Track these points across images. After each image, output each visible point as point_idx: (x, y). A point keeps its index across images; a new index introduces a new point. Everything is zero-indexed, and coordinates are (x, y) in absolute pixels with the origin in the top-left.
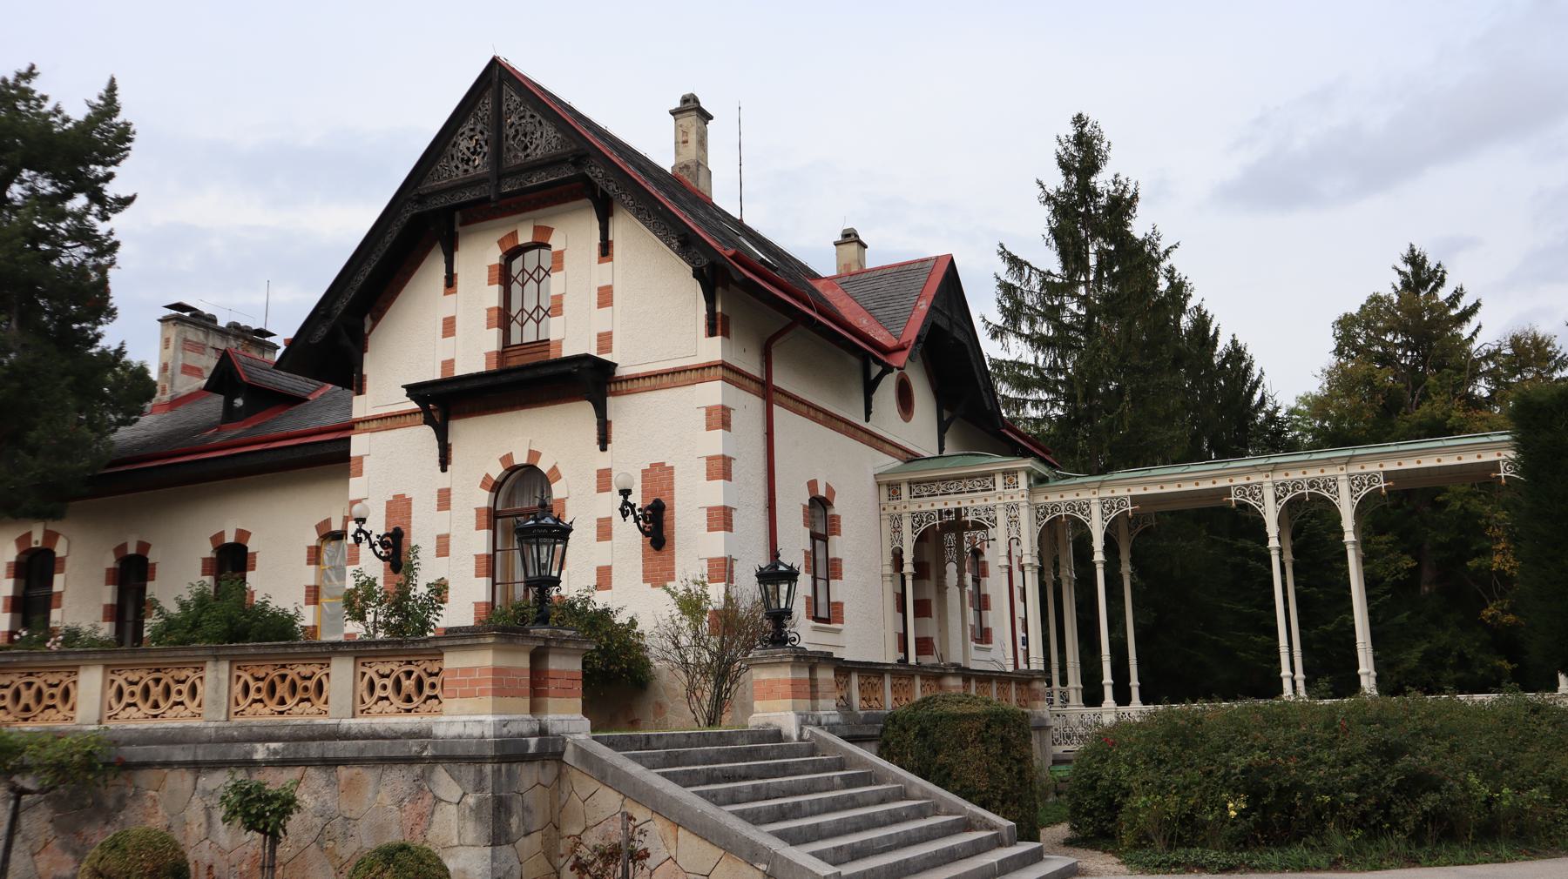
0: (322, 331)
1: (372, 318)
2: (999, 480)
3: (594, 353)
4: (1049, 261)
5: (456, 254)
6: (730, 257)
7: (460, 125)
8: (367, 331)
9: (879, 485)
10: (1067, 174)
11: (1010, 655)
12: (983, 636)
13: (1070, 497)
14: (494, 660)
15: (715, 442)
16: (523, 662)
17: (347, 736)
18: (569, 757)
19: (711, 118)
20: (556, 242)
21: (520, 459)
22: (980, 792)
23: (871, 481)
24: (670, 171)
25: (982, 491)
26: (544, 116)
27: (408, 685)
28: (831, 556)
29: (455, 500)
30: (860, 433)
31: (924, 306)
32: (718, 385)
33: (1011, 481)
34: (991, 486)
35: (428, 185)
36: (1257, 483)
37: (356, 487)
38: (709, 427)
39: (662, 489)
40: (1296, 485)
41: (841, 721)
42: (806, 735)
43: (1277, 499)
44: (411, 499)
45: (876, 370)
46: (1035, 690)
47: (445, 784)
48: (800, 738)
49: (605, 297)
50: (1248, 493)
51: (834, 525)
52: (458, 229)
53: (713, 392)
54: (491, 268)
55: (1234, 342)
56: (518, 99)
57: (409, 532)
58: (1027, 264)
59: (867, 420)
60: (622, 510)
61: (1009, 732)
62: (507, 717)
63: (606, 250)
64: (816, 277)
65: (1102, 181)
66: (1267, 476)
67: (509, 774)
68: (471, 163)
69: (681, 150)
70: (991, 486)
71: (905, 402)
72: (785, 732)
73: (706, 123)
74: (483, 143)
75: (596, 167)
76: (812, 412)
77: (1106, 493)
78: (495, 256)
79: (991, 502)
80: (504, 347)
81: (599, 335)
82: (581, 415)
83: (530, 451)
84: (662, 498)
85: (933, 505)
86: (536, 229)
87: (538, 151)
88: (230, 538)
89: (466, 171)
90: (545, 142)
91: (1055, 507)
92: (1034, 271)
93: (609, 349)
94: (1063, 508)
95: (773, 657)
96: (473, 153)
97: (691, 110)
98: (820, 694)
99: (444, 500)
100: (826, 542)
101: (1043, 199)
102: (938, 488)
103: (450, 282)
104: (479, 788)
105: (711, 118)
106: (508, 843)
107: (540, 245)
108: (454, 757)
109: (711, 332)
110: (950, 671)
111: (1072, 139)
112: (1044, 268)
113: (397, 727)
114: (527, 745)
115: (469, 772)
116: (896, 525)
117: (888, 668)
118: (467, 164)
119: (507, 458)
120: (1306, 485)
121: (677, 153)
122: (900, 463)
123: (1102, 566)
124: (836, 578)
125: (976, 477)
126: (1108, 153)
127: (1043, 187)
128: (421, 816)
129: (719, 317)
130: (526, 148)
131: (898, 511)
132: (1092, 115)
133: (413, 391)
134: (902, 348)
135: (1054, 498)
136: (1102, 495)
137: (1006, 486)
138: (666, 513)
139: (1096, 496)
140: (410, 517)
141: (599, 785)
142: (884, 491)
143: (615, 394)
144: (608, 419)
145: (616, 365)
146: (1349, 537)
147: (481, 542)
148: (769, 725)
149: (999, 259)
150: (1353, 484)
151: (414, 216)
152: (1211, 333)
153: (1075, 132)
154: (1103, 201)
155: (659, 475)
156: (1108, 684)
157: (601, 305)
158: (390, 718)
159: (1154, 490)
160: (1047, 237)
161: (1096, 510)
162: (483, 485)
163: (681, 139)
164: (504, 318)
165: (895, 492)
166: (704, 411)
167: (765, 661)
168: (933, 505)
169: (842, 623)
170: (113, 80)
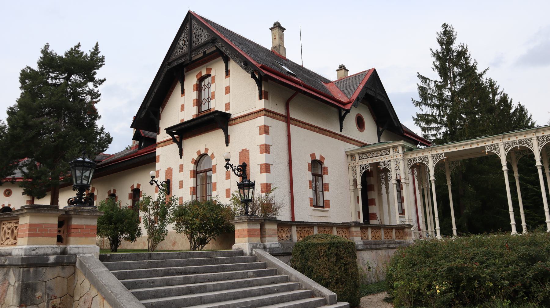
0: (144, 113)
1: (162, 108)
2: (391, 150)
3: (224, 111)
4: (436, 77)
5: (184, 82)
6: (260, 67)
7: (180, 37)
8: (160, 113)
9: (348, 155)
10: (441, 45)
11: (414, 218)
12: (402, 212)
13: (420, 155)
14: (30, 220)
15: (262, 139)
16: (258, 227)
18: (77, 265)
19: (285, 29)
20: (213, 73)
22: (325, 279)
23: (344, 154)
24: (270, 49)
25: (385, 155)
26: (204, 28)
28: (324, 182)
29: (185, 168)
30: (337, 136)
31: (361, 87)
33: (396, 150)
34: (389, 153)
35: (173, 58)
36: (497, 144)
39: (246, 159)
40: (513, 143)
41: (280, 247)
42: (254, 253)
43: (505, 150)
44: (172, 169)
45: (343, 112)
46: (406, 232)
48: (251, 254)
49: (228, 90)
50: (492, 148)
51: (325, 171)
52: (185, 73)
53: (261, 120)
54: (194, 85)
55: (519, 105)
56: (196, 24)
57: (172, 181)
58: (428, 79)
59: (341, 131)
60: (226, 167)
61: (340, 251)
62: (37, 246)
63: (227, 73)
64: (327, 81)
65: (455, 46)
66: (501, 141)
67: (36, 273)
68: (183, 49)
69: (274, 42)
70: (389, 153)
71: (360, 124)
72: (245, 251)
73: (283, 32)
74: (186, 41)
75: (219, 42)
76: (312, 128)
77: (434, 152)
79: (389, 159)
80: (199, 113)
81: (226, 104)
82: (220, 133)
83: (205, 148)
84: (245, 162)
85: (367, 162)
86: (207, 69)
87: (202, 41)
88: (135, 187)
89: (182, 52)
90: (204, 36)
91: (414, 159)
92: (430, 81)
94: (418, 160)
95: (240, 220)
96: (184, 46)
97: (278, 27)
98: (267, 235)
99: (181, 168)
100: (322, 177)
101: (433, 55)
102: (369, 155)
105: (285, 29)
106: (32, 304)
107: (208, 75)
109: (261, 98)
110: (352, 225)
111: (442, 33)
112: (434, 80)
113: (7, 251)
114: (48, 259)
116: (354, 170)
117: (315, 224)
118: (182, 49)
120: (518, 143)
121: (273, 43)
122: (358, 147)
123: (434, 182)
124: (326, 191)
125: (383, 150)
126: (456, 36)
127: (432, 51)
128: (4, 291)
129: (263, 92)
130: (199, 40)
131: (355, 165)
132: (449, 23)
134: (350, 102)
135: (414, 156)
136: (432, 154)
137: (394, 152)
138: (247, 167)
139: (430, 154)
140: (172, 175)
142: (349, 157)
143: (231, 125)
144: (229, 134)
145: (231, 114)
146: (538, 163)
148: (239, 248)
150: (539, 141)
151: (168, 70)
152: (509, 102)
153: (443, 30)
154: (455, 54)
155: (244, 153)
156: (438, 229)
157: (226, 93)
160: (433, 68)
161: (430, 160)
163: (273, 38)
164: (199, 103)
165: (353, 158)
166: (259, 128)
167: (238, 221)
168: (367, 162)
169: (329, 208)
170: (97, 43)
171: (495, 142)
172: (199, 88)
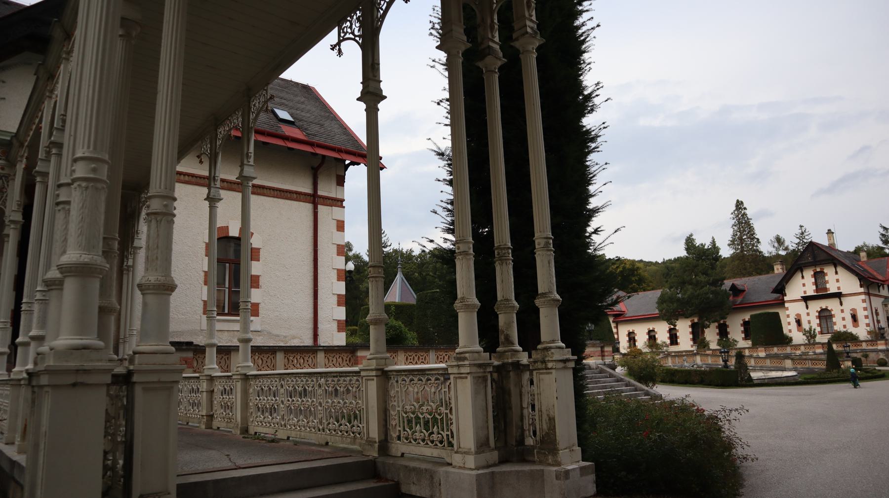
15: (865, 305)
21: (824, 307)
32: (864, 296)
37: (788, 312)
47: (880, 353)
49: (838, 281)
53: (863, 297)
54: (812, 275)
63: (836, 273)
78: (812, 273)
93: (840, 290)
97: (830, 232)
99: (808, 314)
103: (803, 277)
104: (885, 353)
108: (881, 351)
119: (821, 308)
133: (802, 297)
142: (884, 306)
147: (818, 321)
149: (880, 228)
170: (713, 237)
172: (816, 275)
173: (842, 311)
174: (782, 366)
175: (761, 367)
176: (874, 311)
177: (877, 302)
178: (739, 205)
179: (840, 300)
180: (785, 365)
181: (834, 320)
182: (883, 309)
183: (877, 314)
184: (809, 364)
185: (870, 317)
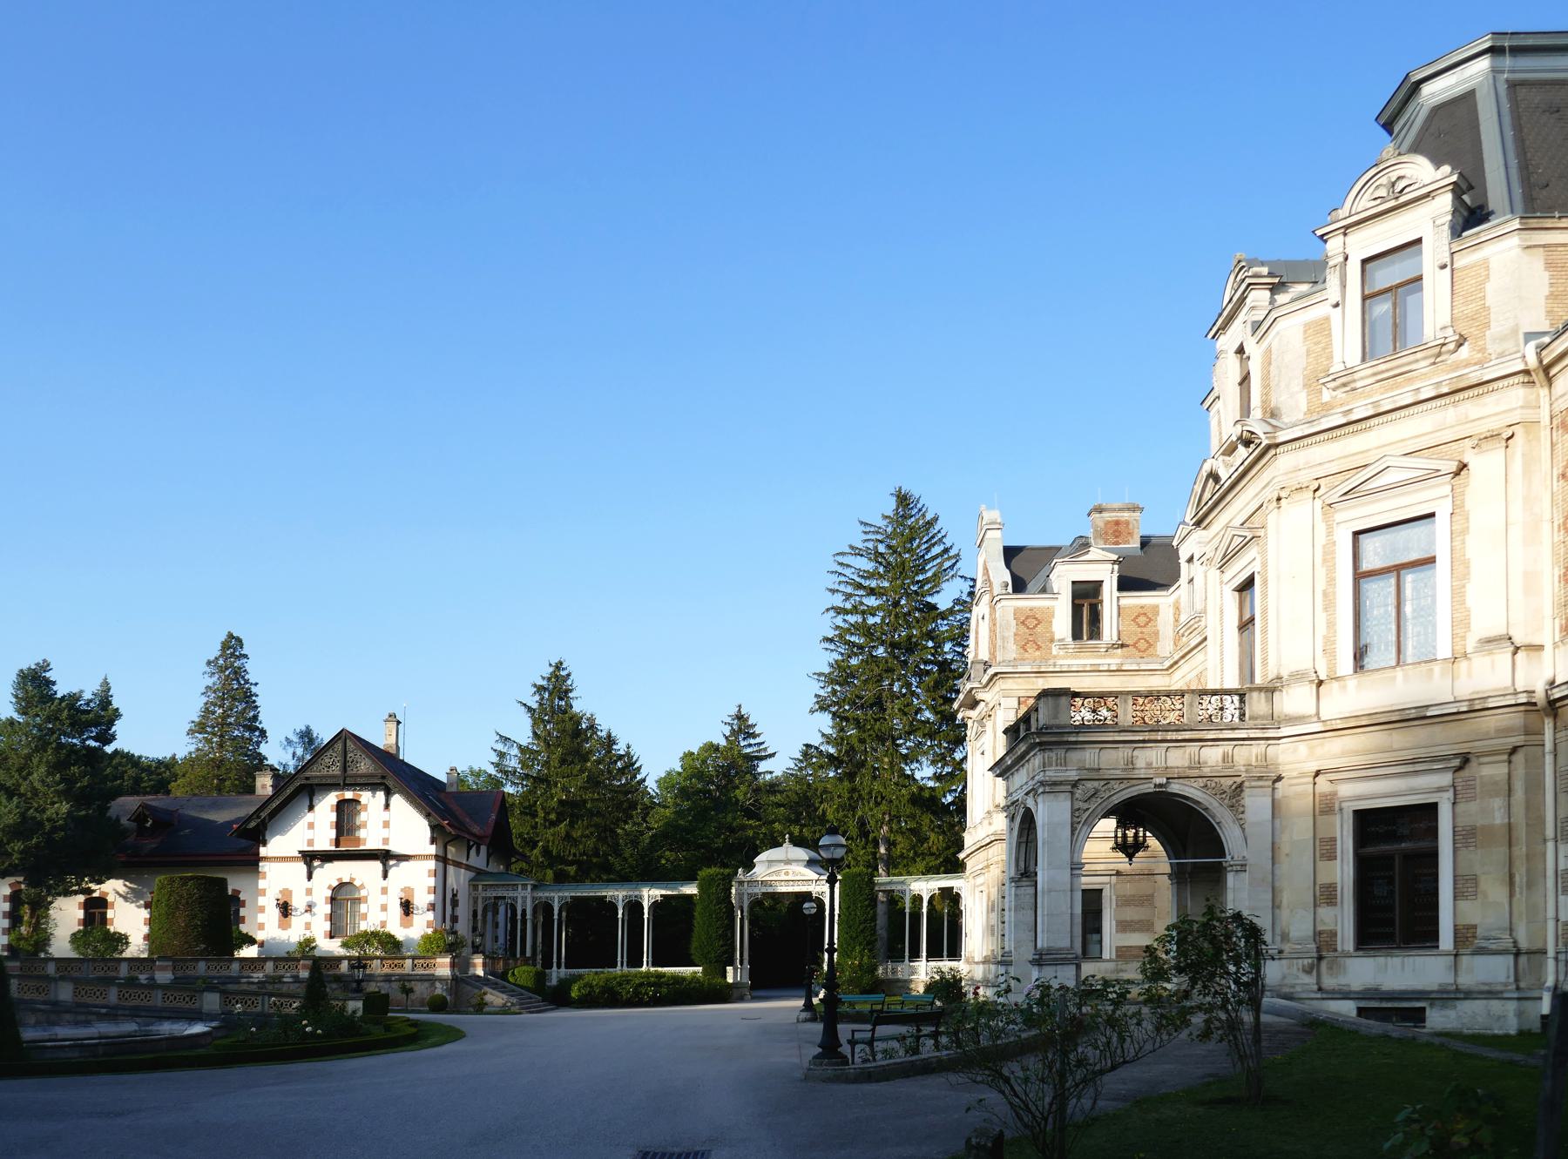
13: (547, 894)
17: (411, 975)
21: (346, 880)
27: (425, 965)
38: (429, 876)
40: (630, 896)
43: (623, 901)
79: (515, 895)
82: (376, 866)
99: (309, 892)
115: (444, 983)
135: (540, 894)
141: (464, 985)
142: (471, 887)
158: (420, 971)
159: (579, 894)
161: (556, 900)
162: (329, 888)
171: (616, 893)
173: (384, 891)
174: (193, 1007)
175: (136, 1008)
176: (449, 896)
177: (458, 879)
178: (232, 646)
179: (385, 865)
180: (202, 1006)
181: (363, 908)
182: (470, 894)
183: (455, 903)
184: (263, 1005)
185: (439, 907)
